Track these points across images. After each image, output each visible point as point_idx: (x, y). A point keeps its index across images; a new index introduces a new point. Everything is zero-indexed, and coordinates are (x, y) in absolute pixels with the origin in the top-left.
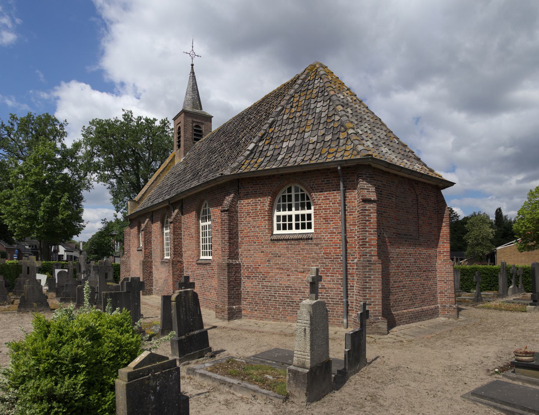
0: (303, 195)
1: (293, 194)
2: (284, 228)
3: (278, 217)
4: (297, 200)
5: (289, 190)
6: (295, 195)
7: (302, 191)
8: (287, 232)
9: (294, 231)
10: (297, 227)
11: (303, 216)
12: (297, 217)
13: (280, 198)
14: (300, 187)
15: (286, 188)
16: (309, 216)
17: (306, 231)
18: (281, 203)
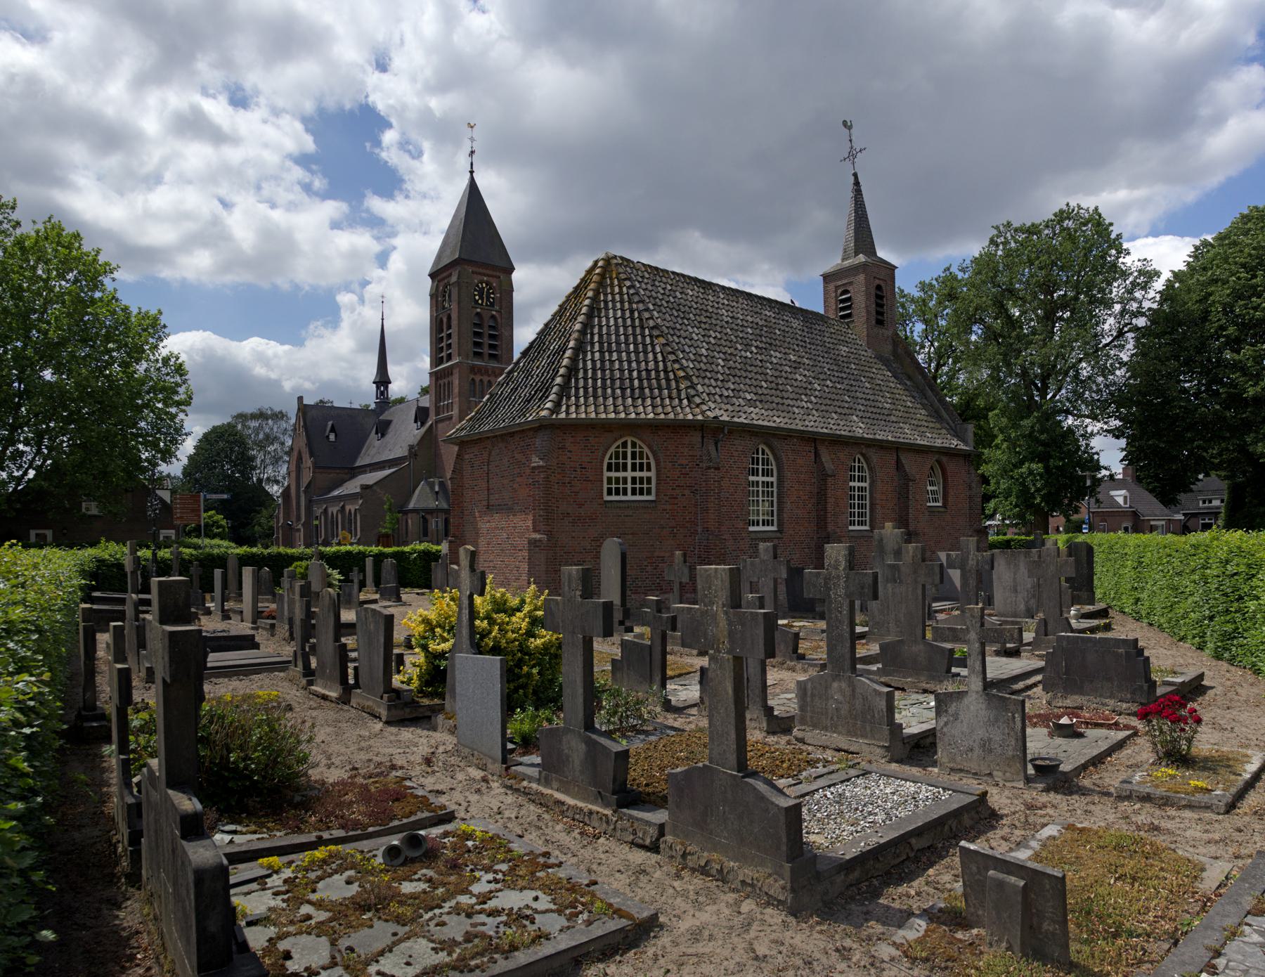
0: (641, 453)
1: (629, 450)
2: (617, 493)
3: (609, 480)
4: (634, 457)
5: (625, 445)
7: (640, 447)
8: (622, 498)
9: (629, 497)
10: (634, 493)
11: (641, 479)
14: (638, 442)
15: (619, 442)
16: (649, 480)
17: (645, 498)
18: (613, 461)
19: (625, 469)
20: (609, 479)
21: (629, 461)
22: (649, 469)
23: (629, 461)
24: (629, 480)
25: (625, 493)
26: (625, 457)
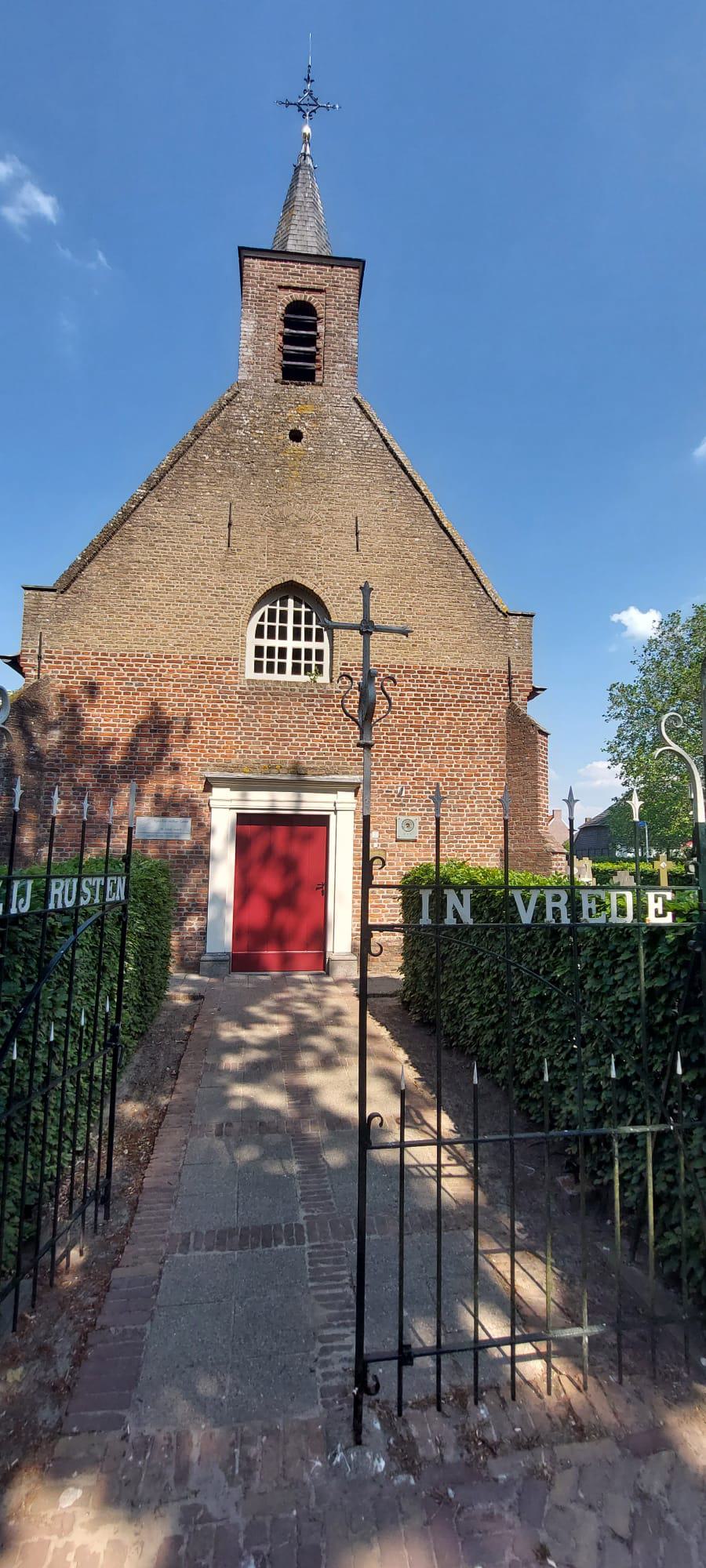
2: (270, 669)
6: (295, 612)
8: (276, 676)
12: (297, 653)
13: (264, 614)
16: (320, 654)
18: (266, 623)
19: (283, 635)
20: (259, 651)
21: (290, 625)
22: (320, 638)
23: (290, 625)
24: (289, 654)
25: (282, 669)
26: (284, 617)
